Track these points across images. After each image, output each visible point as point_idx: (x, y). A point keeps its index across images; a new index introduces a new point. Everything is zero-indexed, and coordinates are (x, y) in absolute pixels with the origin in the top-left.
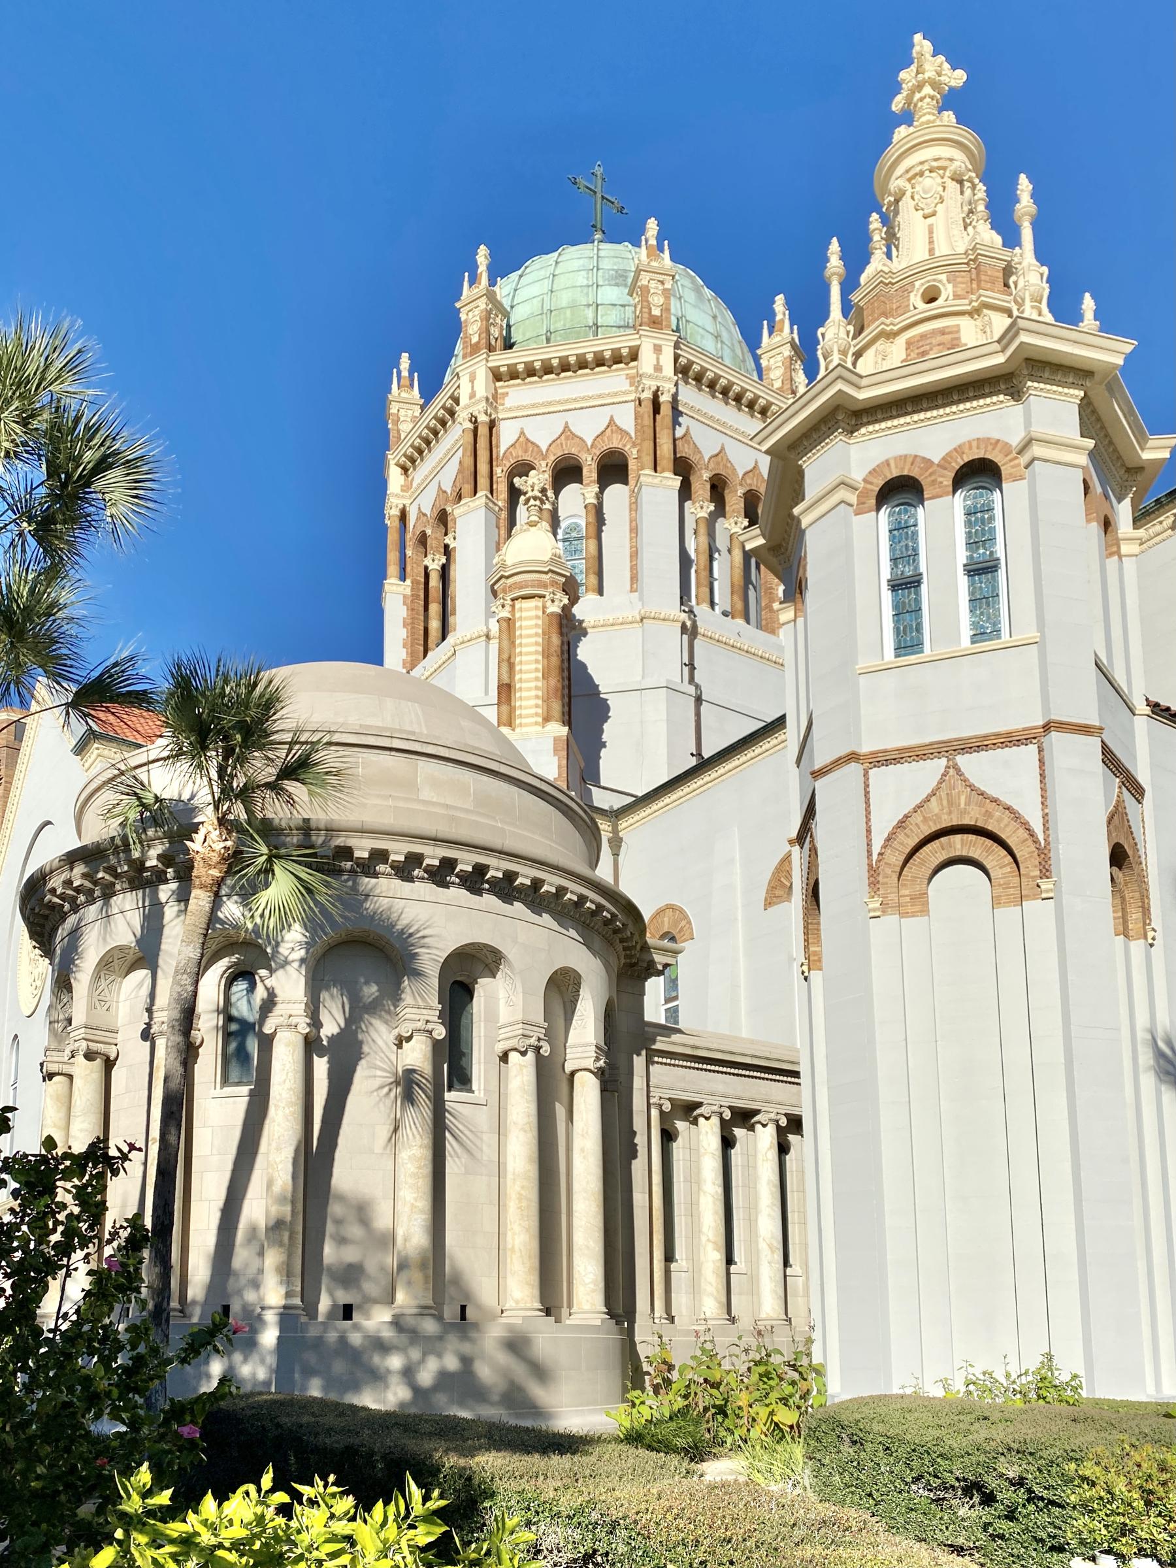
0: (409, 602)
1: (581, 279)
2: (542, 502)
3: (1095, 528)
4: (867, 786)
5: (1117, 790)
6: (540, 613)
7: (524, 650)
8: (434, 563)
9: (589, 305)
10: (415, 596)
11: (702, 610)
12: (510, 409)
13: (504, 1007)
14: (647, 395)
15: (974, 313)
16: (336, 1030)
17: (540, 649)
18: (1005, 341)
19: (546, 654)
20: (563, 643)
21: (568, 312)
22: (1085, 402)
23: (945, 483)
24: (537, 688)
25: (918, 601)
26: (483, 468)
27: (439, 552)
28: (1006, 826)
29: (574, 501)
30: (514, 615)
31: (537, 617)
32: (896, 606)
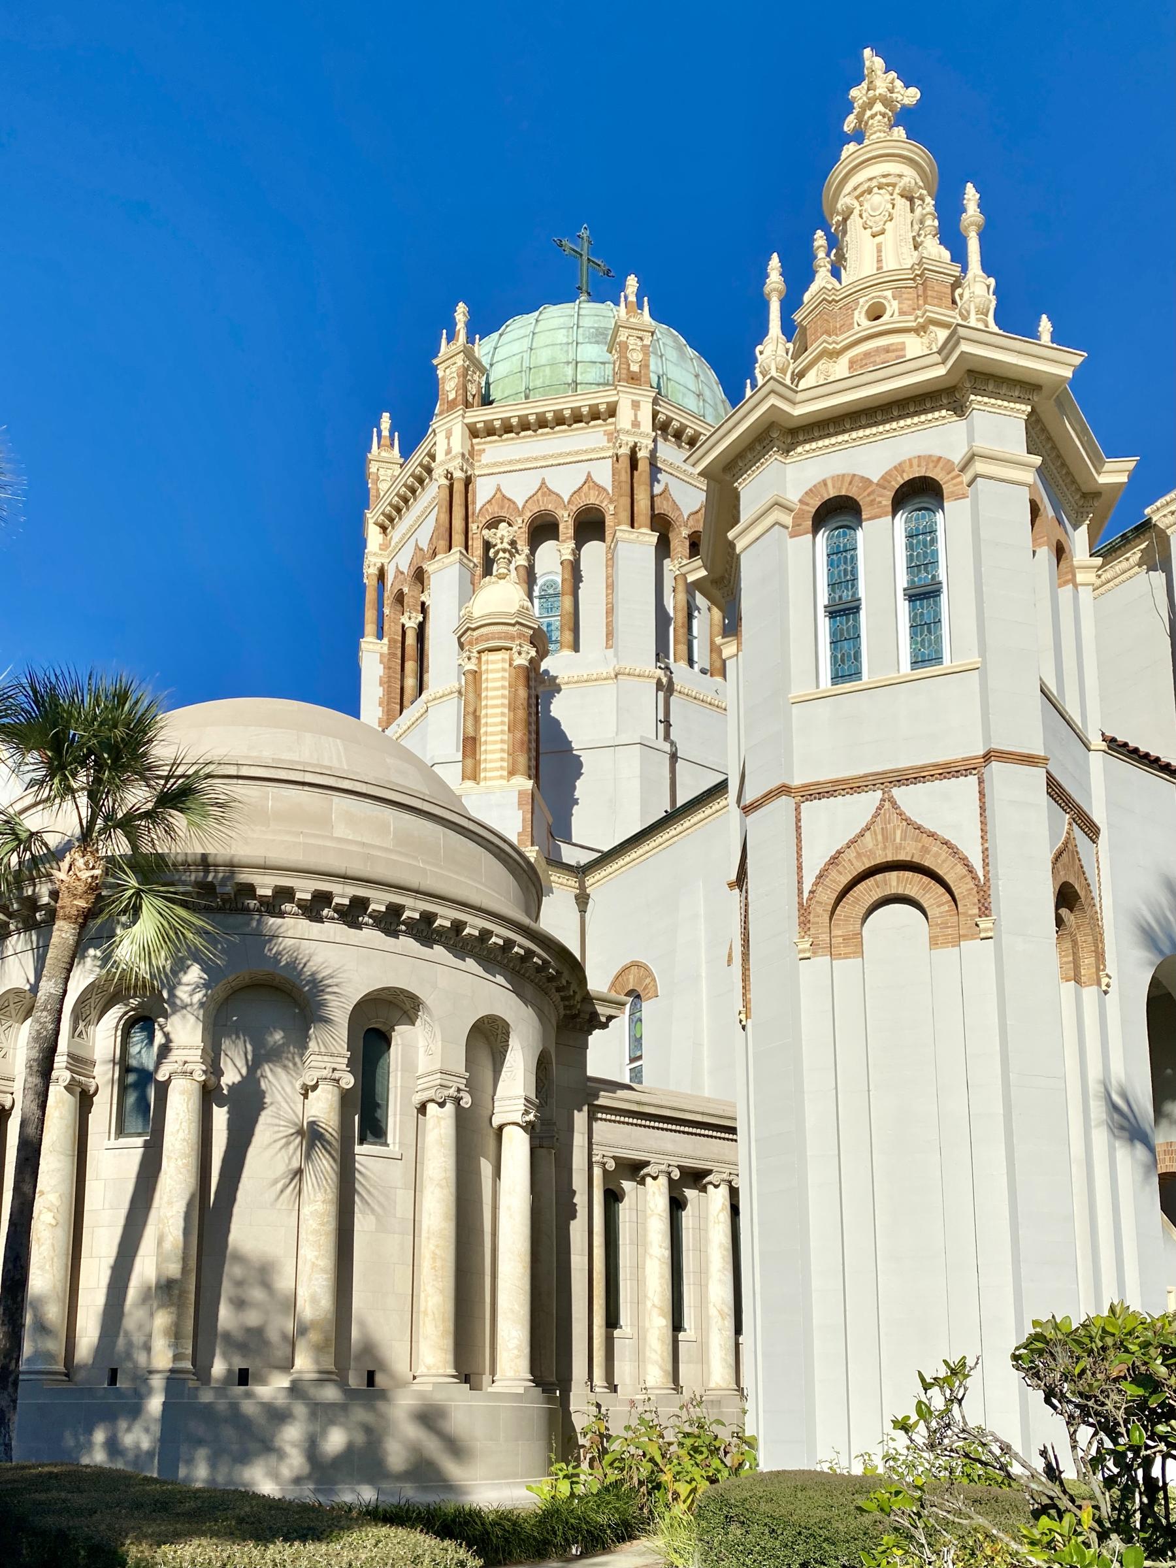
0: (386, 660)
1: (561, 337)
2: (512, 555)
3: (1045, 554)
4: (798, 820)
5: (1066, 827)
6: (507, 666)
7: (490, 702)
8: (411, 621)
9: (568, 363)
10: (392, 654)
11: (679, 668)
12: (487, 465)
13: (421, 1057)
14: (625, 451)
15: (919, 330)
16: (237, 1079)
17: (506, 702)
18: (945, 351)
19: (512, 707)
20: (529, 697)
21: (548, 369)
22: (1033, 418)
23: (884, 503)
24: (502, 741)
25: (856, 628)
26: (458, 524)
27: (416, 611)
28: (944, 861)
29: (551, 558)
30: (480, 668)
31: (504, 670)
32: (833, 634)
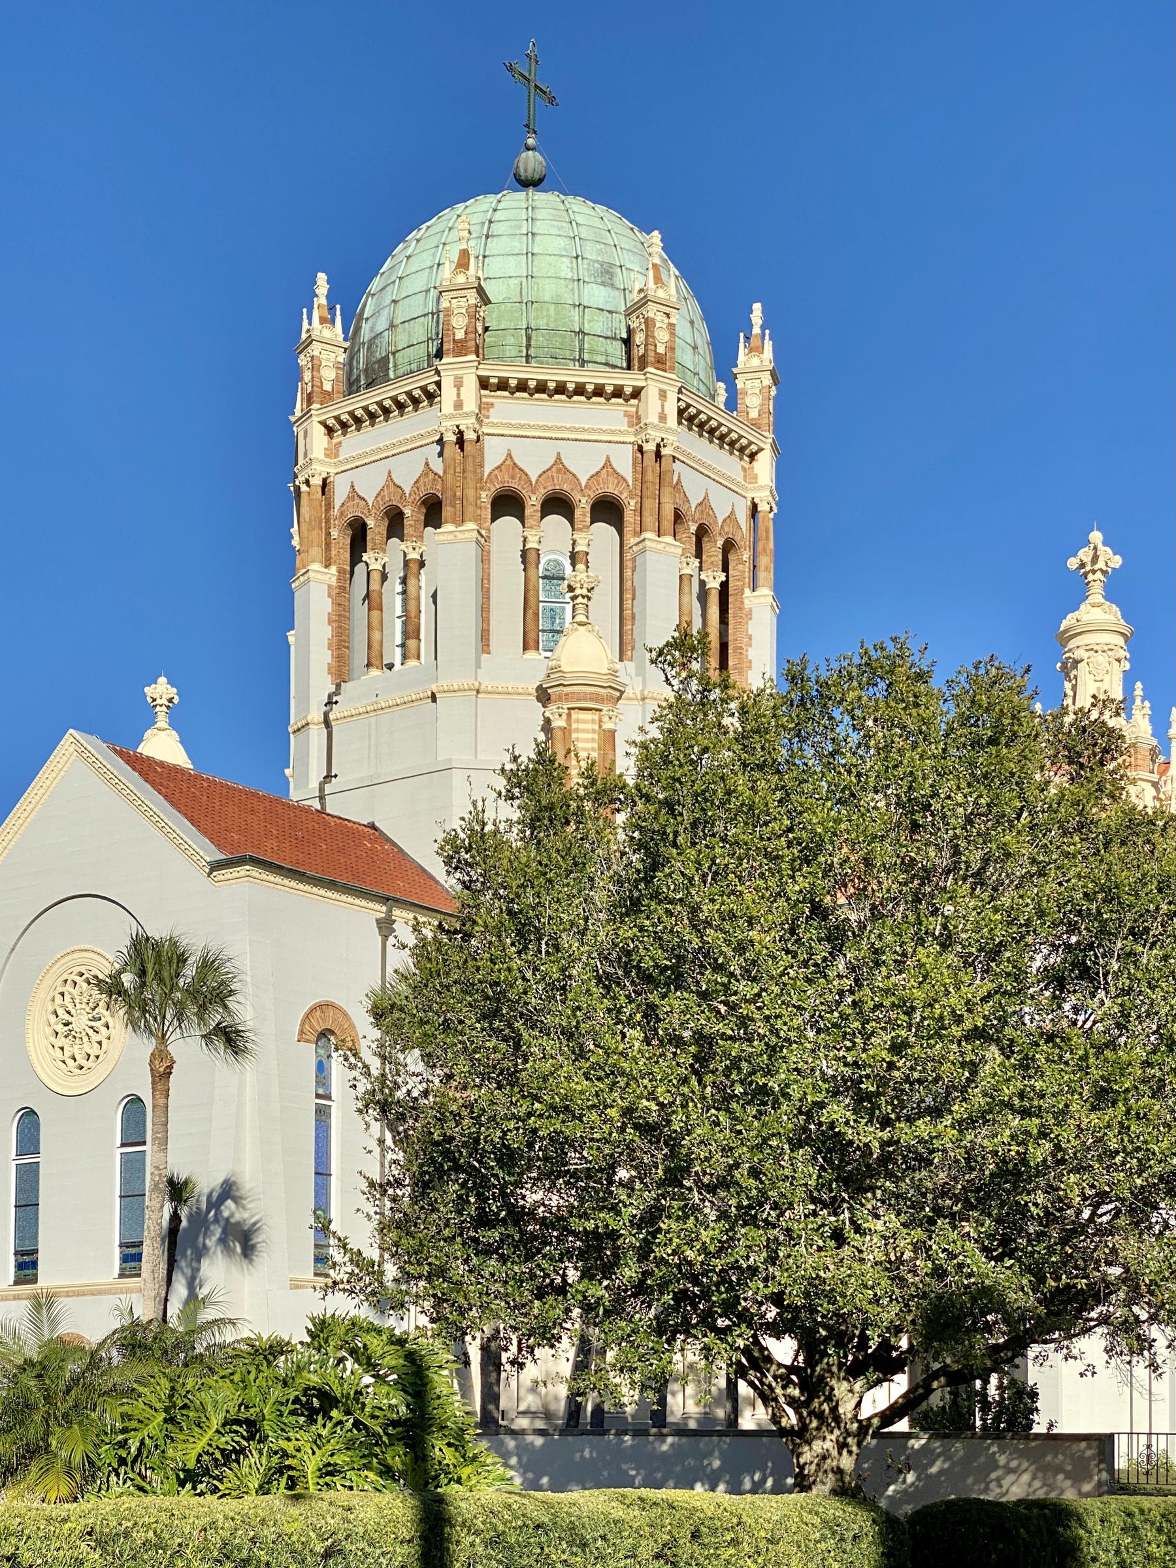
6: (597, 727)
30: (570, 725)
31: (594, 731)
